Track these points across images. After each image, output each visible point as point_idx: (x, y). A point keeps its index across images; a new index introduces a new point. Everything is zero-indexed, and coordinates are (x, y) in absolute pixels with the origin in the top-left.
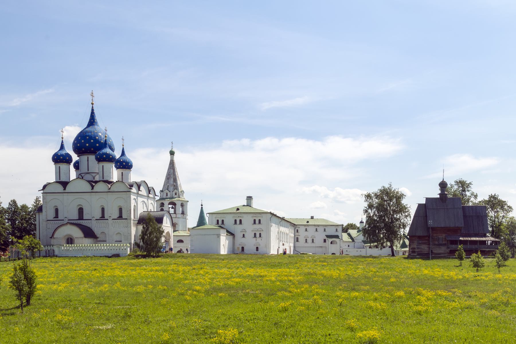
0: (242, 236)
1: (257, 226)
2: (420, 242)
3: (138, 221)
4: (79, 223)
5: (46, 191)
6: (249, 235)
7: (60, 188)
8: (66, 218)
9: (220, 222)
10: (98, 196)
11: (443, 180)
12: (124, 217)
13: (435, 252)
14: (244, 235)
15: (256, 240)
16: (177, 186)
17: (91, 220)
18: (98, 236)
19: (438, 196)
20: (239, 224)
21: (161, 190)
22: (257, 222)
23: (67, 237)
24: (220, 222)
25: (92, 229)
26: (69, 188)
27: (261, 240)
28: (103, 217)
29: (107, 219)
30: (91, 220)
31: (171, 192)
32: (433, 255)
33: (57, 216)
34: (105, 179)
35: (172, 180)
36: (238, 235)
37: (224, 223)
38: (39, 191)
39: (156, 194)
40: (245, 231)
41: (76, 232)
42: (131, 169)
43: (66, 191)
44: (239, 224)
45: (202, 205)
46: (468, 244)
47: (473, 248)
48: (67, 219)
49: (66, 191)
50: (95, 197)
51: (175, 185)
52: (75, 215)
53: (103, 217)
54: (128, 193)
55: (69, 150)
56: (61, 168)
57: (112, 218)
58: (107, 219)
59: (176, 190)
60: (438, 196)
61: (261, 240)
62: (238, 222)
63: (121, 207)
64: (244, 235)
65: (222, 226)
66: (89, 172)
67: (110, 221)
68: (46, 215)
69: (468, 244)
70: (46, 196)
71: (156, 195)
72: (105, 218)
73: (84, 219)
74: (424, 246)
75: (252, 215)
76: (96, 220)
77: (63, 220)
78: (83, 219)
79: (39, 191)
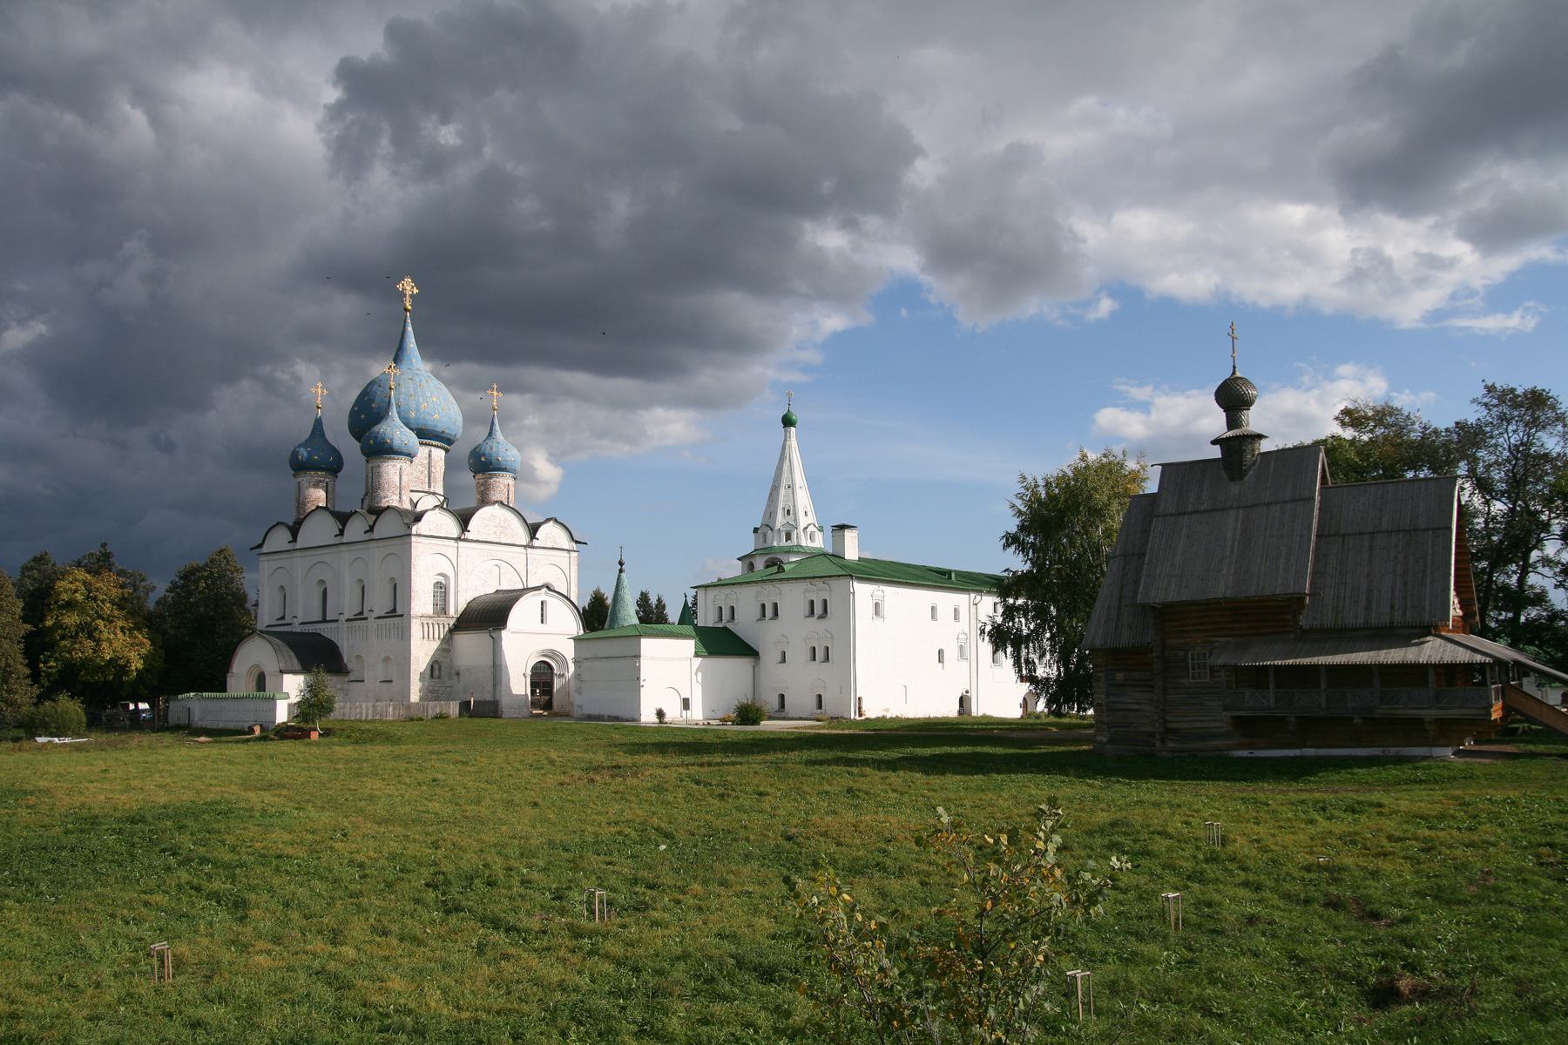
0: (779, 658)
3: (458, 619)
5: (265, 549)
6: (798, 655)
8: (295, 620)
11: (1234, 373)
12: (399, 612)
13: (1186, 725)
14: (784, 654)
17: (337, 621)
18: (350, 666)
19: (1216, 452)
21: (755, 528)
24: (726, 615)
25: (338, 647)
29: (366, 619)
32: (1171, 745)
33: (283, 618)
36: (769, 656)
37: (736, 617)
39: (575, 539)
45: (621, 564)
46: (1323, 685)
50: (346, 555)
54: (406, 539)
58: (366, 619)
60: (1216, 452)
65: (730, 626)
67: (372, 623)
69: (1323, 685)
72: (398, 613)
75: (802, 585)
76: (348, 620)
78: (324, 621)
79: (252, 549)
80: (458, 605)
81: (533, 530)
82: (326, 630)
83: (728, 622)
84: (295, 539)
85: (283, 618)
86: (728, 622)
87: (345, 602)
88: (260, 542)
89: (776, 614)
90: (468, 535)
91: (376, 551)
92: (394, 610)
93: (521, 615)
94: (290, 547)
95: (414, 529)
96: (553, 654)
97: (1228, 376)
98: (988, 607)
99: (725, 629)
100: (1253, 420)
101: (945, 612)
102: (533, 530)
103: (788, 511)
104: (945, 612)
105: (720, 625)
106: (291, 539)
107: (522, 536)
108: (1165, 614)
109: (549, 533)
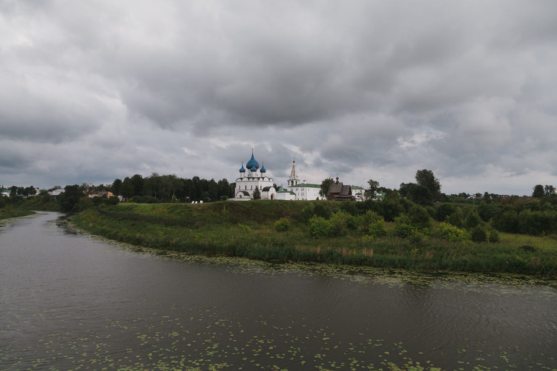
1: (302, 192)
7: (240, 180)
10: (250, 182)
22: (303, 190)
26: (243, 180)
28: (251, 189)
34: (253, 177)
36: (297, 195)
41: (242, 194)
50: (249, 183)
53: (251, 189)
55: (245, 168)
80: (262, 188)
81: (269, 179)
82: (246, 191)
87: (249, 188)
91: (254, 183)
93: (270, 189)
95: (259, 180)
96: (273, 194)
98: (319, 189)
100: (339, 180)
101: (315, 190)
102: (269, 179)
104: (315, 190)
107: (268, 180)
108: (332, 193)
109: (271, 180)
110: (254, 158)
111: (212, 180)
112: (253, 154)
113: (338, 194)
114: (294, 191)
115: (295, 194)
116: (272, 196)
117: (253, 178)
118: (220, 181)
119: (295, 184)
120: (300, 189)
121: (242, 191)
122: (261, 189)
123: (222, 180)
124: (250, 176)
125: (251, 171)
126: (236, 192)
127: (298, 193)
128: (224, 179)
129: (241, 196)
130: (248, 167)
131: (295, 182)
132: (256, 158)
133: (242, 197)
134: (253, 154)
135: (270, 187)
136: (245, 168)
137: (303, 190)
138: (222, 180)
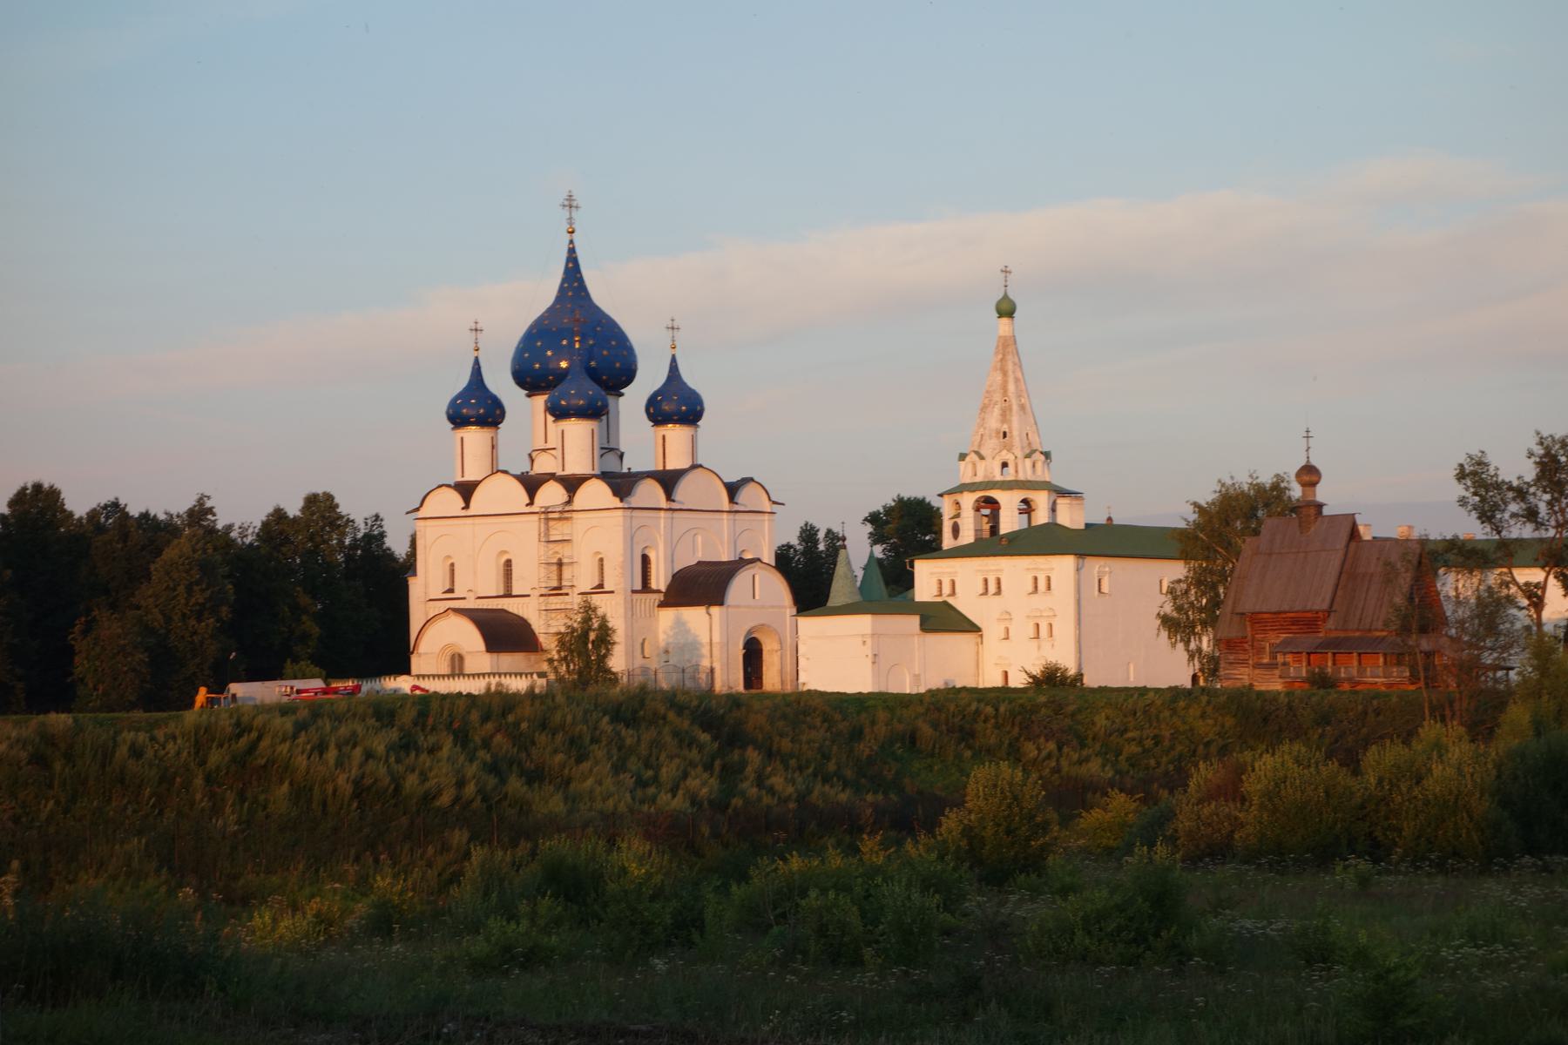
1: (1040, 601)
2: (1232, 657)
4: (500, 607)
5: (420, 514)
6: (1022, 629)
8: (471, 594)
9: (946, 589)
14: (1007, 630)
15: (1039, 648)
16: (1011, 437)
20: (994, 594)
22: (1042, 584)
23: (449, 653)
24: (946, 589)
27: (1053, 645)
29: (567, 594)
30: (528, 596)
31: (989, 459)
33: (451, 591)
35: (997, 411)
36: (992, 631)
38: (408, 513)
40: (1008, 617)
41: (470, 639)
42: (699, 423)
43: (471, 512)
44: (994, 594)
47: (1343, 675)
48: (471, 597)
49: (471, 512)
51: (1007, 430)
52: (493, 585)
56: (465, 440)
57: (577, 591)
59: (1004, 452)
61: (1053, 645)
62: (992, 588)
63: (600, 556)
64: (1007, 630)
65: (951, 601)
66: (547, 447)
68: (426, 586)
70: (425, 526)
71: (774, 503)
73: (514, 593)
74: (1243, 670)
77: (464, 598)
79: (408, 513)
80: (660, 580)
82: (511, 605)
83: (949, 596)
84: (467, 507)
85: (451, 591)
86: (949, 596)
88: (418, 506)
89: (999, 592)
90: (674, 506)
92: (601, 586)
93: (738, 587)
94: (464, 513)
97: (1303, 463)
99: (945, 603)
102: (733, 490)
103: (1005, 435)
105: (939, 599)
106: (463, 505)
109: (746, 496)
110: (581, 280)
111: (200, 513)
112: (572, 258)
113: (1307, 622)
114: (967, 603)
115: (973, 628)
116: (753, 653)
117: (572, 484)
118: (279, 515)
119: (1010, 522)
120: (1015, 570)
121: (471, 604)
122: (646, 587)
123: (294, 509)
124: (545, 465)
125: (550, 418)
126: (418, 613)
127: (1007, 616)
128: (312, 501)
129: (461, 658)
130: (530, 378)
131: (1009, 503)
132: (603, 292)
133: (469, 667)
134: (572, 251)
135: (740, 564)
136: (501, 383)
137: (1042, 584)
138: (294, 509)
